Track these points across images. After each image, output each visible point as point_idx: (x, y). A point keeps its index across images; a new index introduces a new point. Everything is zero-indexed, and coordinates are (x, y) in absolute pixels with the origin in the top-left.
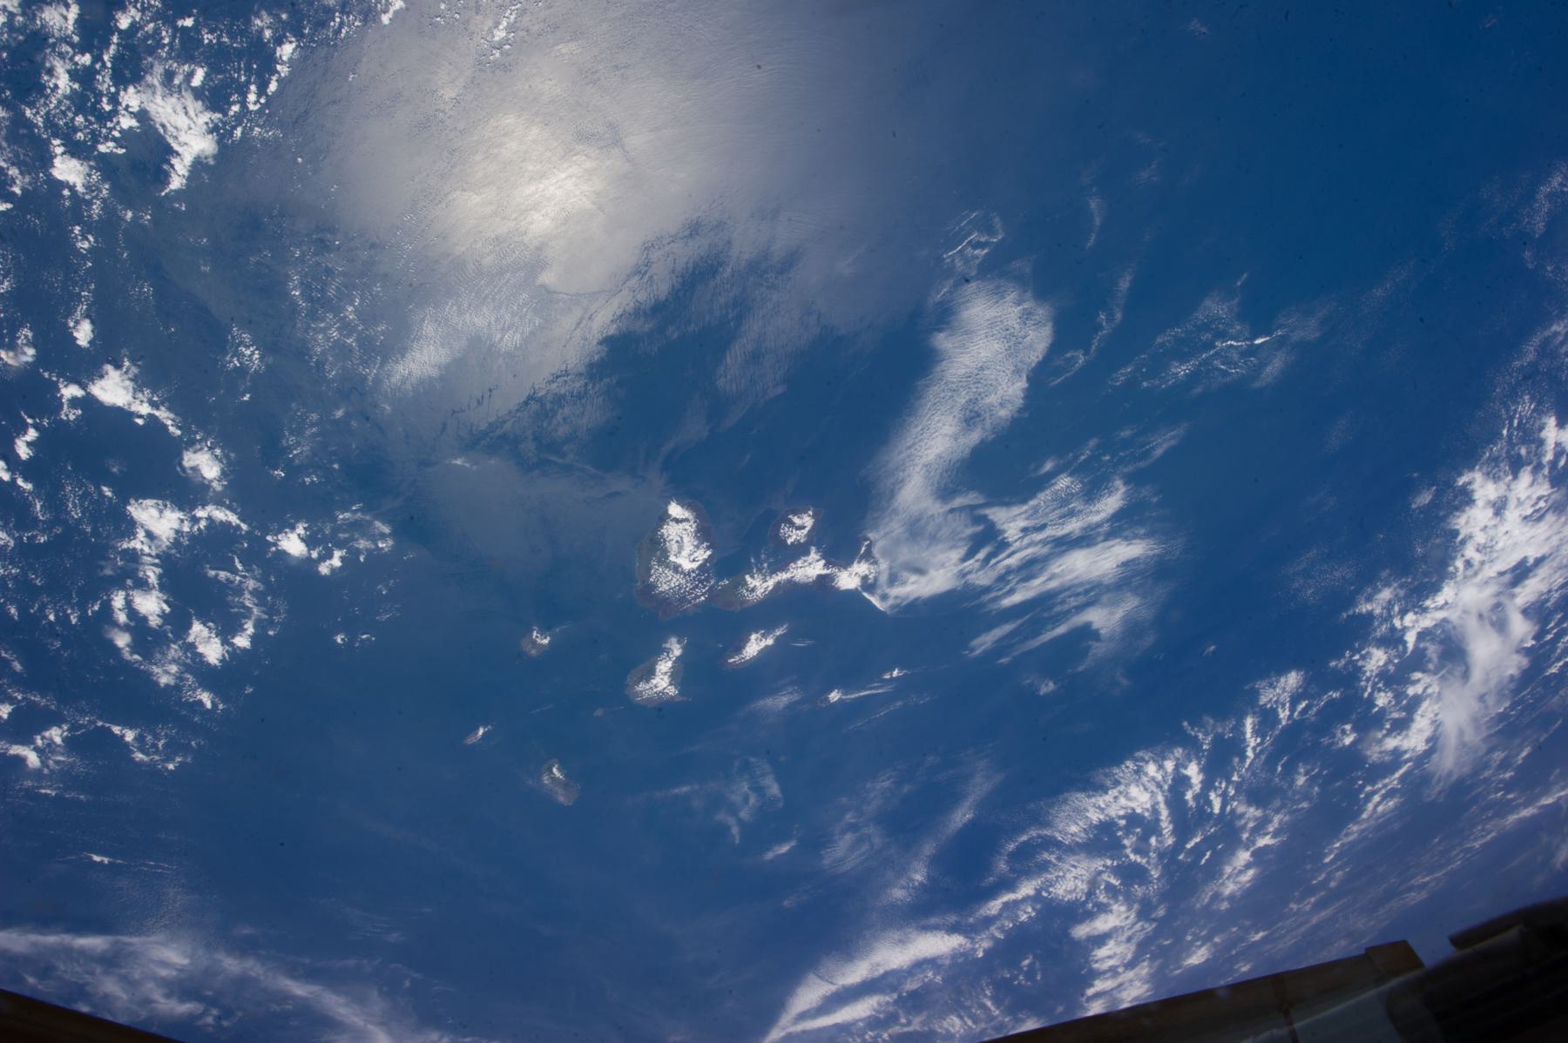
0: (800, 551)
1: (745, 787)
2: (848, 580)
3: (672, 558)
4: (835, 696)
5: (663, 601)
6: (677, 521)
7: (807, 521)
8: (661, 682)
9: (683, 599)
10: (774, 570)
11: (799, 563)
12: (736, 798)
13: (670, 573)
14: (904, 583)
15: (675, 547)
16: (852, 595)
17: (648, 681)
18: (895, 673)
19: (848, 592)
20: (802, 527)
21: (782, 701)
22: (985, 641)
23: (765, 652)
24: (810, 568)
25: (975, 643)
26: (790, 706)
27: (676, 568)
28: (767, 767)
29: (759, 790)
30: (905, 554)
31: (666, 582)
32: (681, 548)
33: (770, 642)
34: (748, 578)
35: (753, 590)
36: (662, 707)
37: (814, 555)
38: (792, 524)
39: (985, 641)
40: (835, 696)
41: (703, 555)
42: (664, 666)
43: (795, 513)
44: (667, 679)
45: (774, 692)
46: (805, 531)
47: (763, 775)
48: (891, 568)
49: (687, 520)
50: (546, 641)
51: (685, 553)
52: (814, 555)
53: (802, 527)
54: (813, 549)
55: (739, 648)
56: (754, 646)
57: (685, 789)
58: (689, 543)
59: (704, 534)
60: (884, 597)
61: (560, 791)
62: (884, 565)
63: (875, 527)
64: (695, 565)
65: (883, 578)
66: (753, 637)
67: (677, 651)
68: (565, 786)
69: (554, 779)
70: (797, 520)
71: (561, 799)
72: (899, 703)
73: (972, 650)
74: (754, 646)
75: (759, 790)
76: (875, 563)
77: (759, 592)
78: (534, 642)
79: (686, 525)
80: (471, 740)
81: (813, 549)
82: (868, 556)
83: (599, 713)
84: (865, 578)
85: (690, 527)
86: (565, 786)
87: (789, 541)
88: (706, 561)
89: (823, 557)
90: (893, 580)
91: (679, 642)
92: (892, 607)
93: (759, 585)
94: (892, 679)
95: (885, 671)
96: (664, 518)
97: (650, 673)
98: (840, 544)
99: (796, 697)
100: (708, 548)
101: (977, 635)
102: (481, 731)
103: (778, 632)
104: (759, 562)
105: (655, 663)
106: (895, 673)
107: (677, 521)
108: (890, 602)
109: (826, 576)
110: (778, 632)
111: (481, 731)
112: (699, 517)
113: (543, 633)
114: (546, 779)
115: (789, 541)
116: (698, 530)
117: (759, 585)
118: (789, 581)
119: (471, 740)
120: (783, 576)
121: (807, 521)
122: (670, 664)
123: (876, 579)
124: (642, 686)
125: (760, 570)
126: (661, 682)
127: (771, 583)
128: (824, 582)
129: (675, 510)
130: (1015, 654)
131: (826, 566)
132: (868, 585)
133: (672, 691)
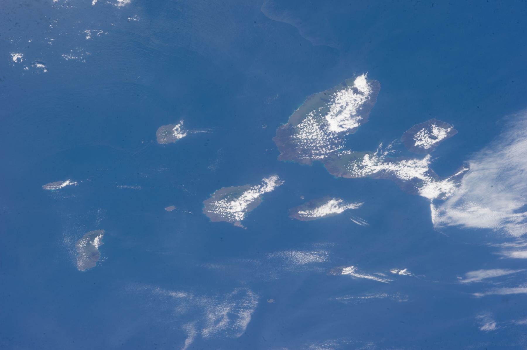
0: (420, 153)
1: (225, 311)
2: (430, 191)
3: (328, 118)
4: (348, 271)
5: (293, 146)
6: (356, 91)
7: (441, 134)
8: (237, 208)
9: (307, 151)
10: (387, 160)
11: (410, 162)
12: (212, 317)
13: (316, 126)
14: (464, 210)
15: (338, 109)
16: (425, 202)
17: (229, 201)
18: (402, 272)
19: (425, 198)
20: (435, 138)
21: (305, 258)
22: (479, 275)
23: (330, 219)
24: (411, 170)
25: (471, 273)
26: (310, 265)
27: (324, 126)
28: (255, 303)
29: (233, 317)
30: (482, 189)
31: (309, 132)
32: (340, 112)
33: (340, 211)
34: (366, 157)
35: (362, 167)
36: (225, 226)
37: (425, 162)
38: (430, 131)
39: (479, 275)
40: (348, 271)
41: (352, 124)
42: (251, 195)
43: (438, 125)
44: (244, 205)
45: (307, 248)
46: (434, 141)
47: (246, 308)
48: (464, 195)
49: (362, 94)
50: (180, 136)
51: (340, 117)
52: (425, 162)
53: (435, 138)
54: (428, 156)
55: (313, 206)
56: (329, 208)
57: (181, 295)
58: (351, 109)
59: (363, 111)
60: (442, 214)
61: (85, 257)
62: (462, 190)
63: (480, 160)
64: (340, 130)
65: (454, 200)
66: (332, 202)
67: (270, 185)
68: (93, 254)
69: (89, 245)
70: (435, 131)
71: (80, 264)
72: (385, 295)
73: (465, 278)
74: (329, 208)
75: (233, 317)
76: (457, 186)
77: (364, 172)
78: (171, 132)
79: (358, 97)
80: (50, 187)
81: (428, 156)
82: (457, 180)
83: (170, 209)
84: (443, 194)
85: (360, 100)
86: (93, 254)
87: (417, 143)
88: (349, 130)
89: (430, 166)
90: (460, 204)
91: (276, 182)
92: (442, 224)
93: (370, 165)
94: (397, 275)
95: (394, 267)
96: (346, 82)
97: (236, 195)
98: (445, 164)
99: (320, 260)
100: (359, 121)
101: (477, 268)
102: (67, 183)
103: (351, 207)
104: (384, 148)
105: (246, 190)
106: (402, 272)
107: (356, 91)
108: (443, 219)
109: (421, 180)
110: (351, 207)
111: (67, 183)
112: (372, 96)
113: (183, 129)
114: (82, 244)
115: (417, 143)
116: (364, 105)
117: (370, 165)
118: (392, 175)
119: (50, 187)
120: (391, 167)
121: (441, 134)
122: (256, 195)
123: (448, 199)
124: (221, 203)
125: (379, 155)
126: (237, 208)
127: (379, 168)
128: (416, 183)
129: (361, 82)
130: (489, 293)
131: (426, 174)
132: (439, 202)
133: (240, 217)
